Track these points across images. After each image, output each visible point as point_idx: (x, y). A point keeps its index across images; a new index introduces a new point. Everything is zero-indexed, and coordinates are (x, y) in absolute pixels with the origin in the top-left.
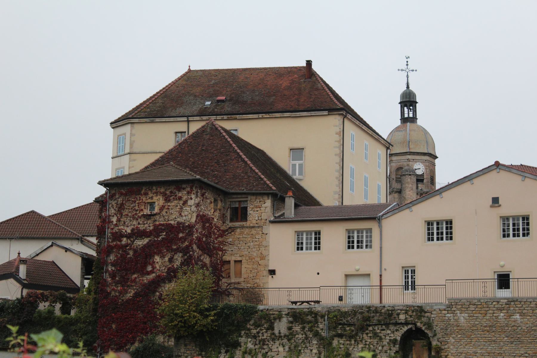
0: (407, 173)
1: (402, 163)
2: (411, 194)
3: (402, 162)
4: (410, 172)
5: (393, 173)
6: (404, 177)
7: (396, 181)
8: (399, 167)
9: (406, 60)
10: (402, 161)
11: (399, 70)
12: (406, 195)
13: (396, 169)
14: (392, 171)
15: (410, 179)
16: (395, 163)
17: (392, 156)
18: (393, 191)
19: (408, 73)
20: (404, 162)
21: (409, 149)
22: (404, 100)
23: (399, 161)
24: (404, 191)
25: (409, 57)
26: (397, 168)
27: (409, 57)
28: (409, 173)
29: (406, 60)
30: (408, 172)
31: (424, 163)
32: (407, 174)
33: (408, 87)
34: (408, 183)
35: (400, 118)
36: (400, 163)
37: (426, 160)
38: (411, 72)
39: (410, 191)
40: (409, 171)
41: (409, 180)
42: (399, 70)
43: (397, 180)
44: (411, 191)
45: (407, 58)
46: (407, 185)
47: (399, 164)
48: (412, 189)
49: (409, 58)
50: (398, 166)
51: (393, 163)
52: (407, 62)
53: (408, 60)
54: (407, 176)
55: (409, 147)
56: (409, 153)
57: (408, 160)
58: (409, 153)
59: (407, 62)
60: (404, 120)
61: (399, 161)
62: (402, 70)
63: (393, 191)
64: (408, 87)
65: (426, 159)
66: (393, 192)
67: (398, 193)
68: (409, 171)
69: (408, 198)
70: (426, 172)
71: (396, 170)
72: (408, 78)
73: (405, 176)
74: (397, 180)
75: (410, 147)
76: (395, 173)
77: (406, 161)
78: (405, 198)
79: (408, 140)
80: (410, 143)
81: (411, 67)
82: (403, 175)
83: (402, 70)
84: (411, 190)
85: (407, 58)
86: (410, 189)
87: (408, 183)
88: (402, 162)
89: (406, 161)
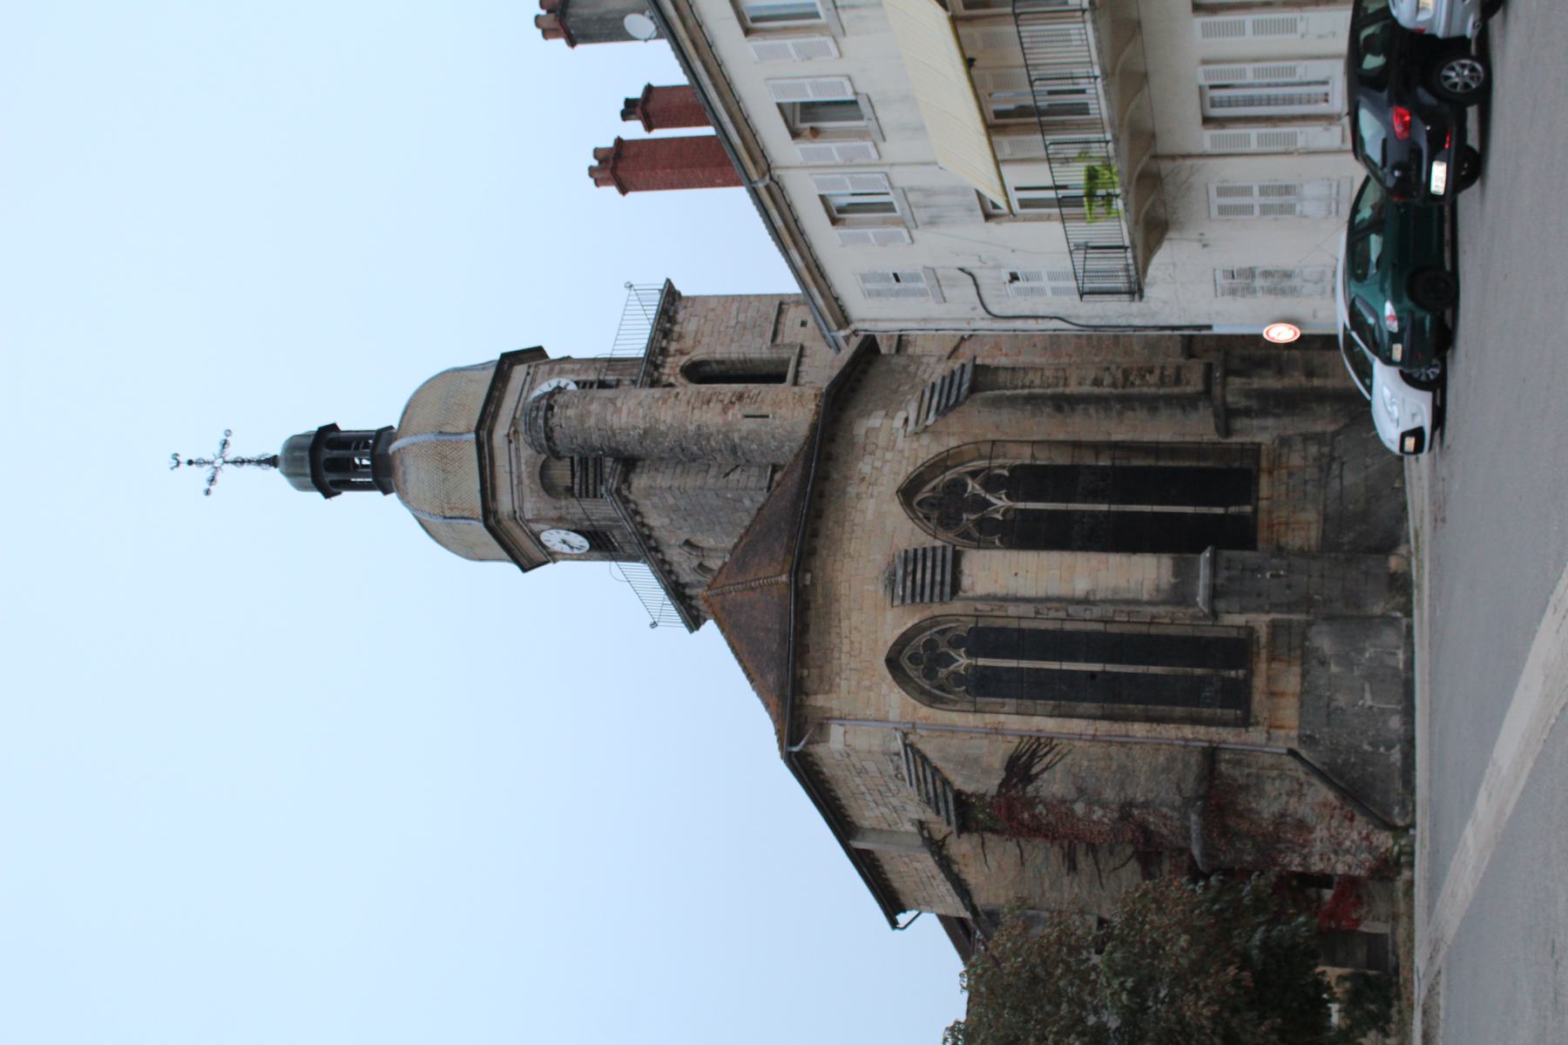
0: (541, 422)
1: (523, 467)
2: (632, 403)
3: (519, 468)
4: (538, 409)
5: (563, 512)
6: (557, 434)
7: (595, 496)
8: (538, 481)
9: (184, 466)
10: (514, 470)
11: (208, 492)
12: (635, 428)
13: (547, 497)
14: (553, 514)
15: (567, 407)
16: (522, 500)
17: (496, 513)
18: (618, 491)
19: (227, 459)
20: (518, 458)
21: (469, 432)
22: (308, 471)
23: (515, 482)
24: (614, 435)
25: (175, 456)
26: (542, 493)
27: (175, 456)
28: (541, 413)
29: (184, 466)
30: (536, 418)
31: (537, 381)
32: (546, 420)
33: (272, 461)
34: (582, 418)
35: (378, 494)
36: (524, 475)
37: (528, 374)
38: (227, 451)
39: (618, 411)
40: (534, 414)
41: (570, 412)
42: (208, 492)
43: (591, 492)
44: (619, 404)
45: (178, 463)
46: (591, 422)
47: (526, 481)
48: (612, 401)
49: (177, 455)
50: (537, 486)
51: (521, 509)
52: (190, 462)
53: (183, 459)
54: (554, 421)
55: (461, 434)
56: (484, 434)
57: (510, 442)
58: (484, 434)
59: (190, 462)
60: (382, 478)
61: (515, 482)
62: (212, 480)
63: (618, 491)
64: (272, 461)
65: (525, 374)
66: (625, 493)
67: (632, 475)
68: (534, 414)
69: (644, 417)
70: (573, 371)
71: (550, 495)
72: (243, 462)
73: (552, 430)
74: (591, 492)
75: (461, 429)
76: (563, 503)
77: (517, 449)
78: (646, 432)
79: (432, 438)
80: (448, 429)
81: (210, 451)
82: (549, 438)
83: (212, 480)
84: (615, 404)
85: (179, 463)
86: (611, 408)
87: (582, 418)
88: (519, 468)
89: (517, 449)
